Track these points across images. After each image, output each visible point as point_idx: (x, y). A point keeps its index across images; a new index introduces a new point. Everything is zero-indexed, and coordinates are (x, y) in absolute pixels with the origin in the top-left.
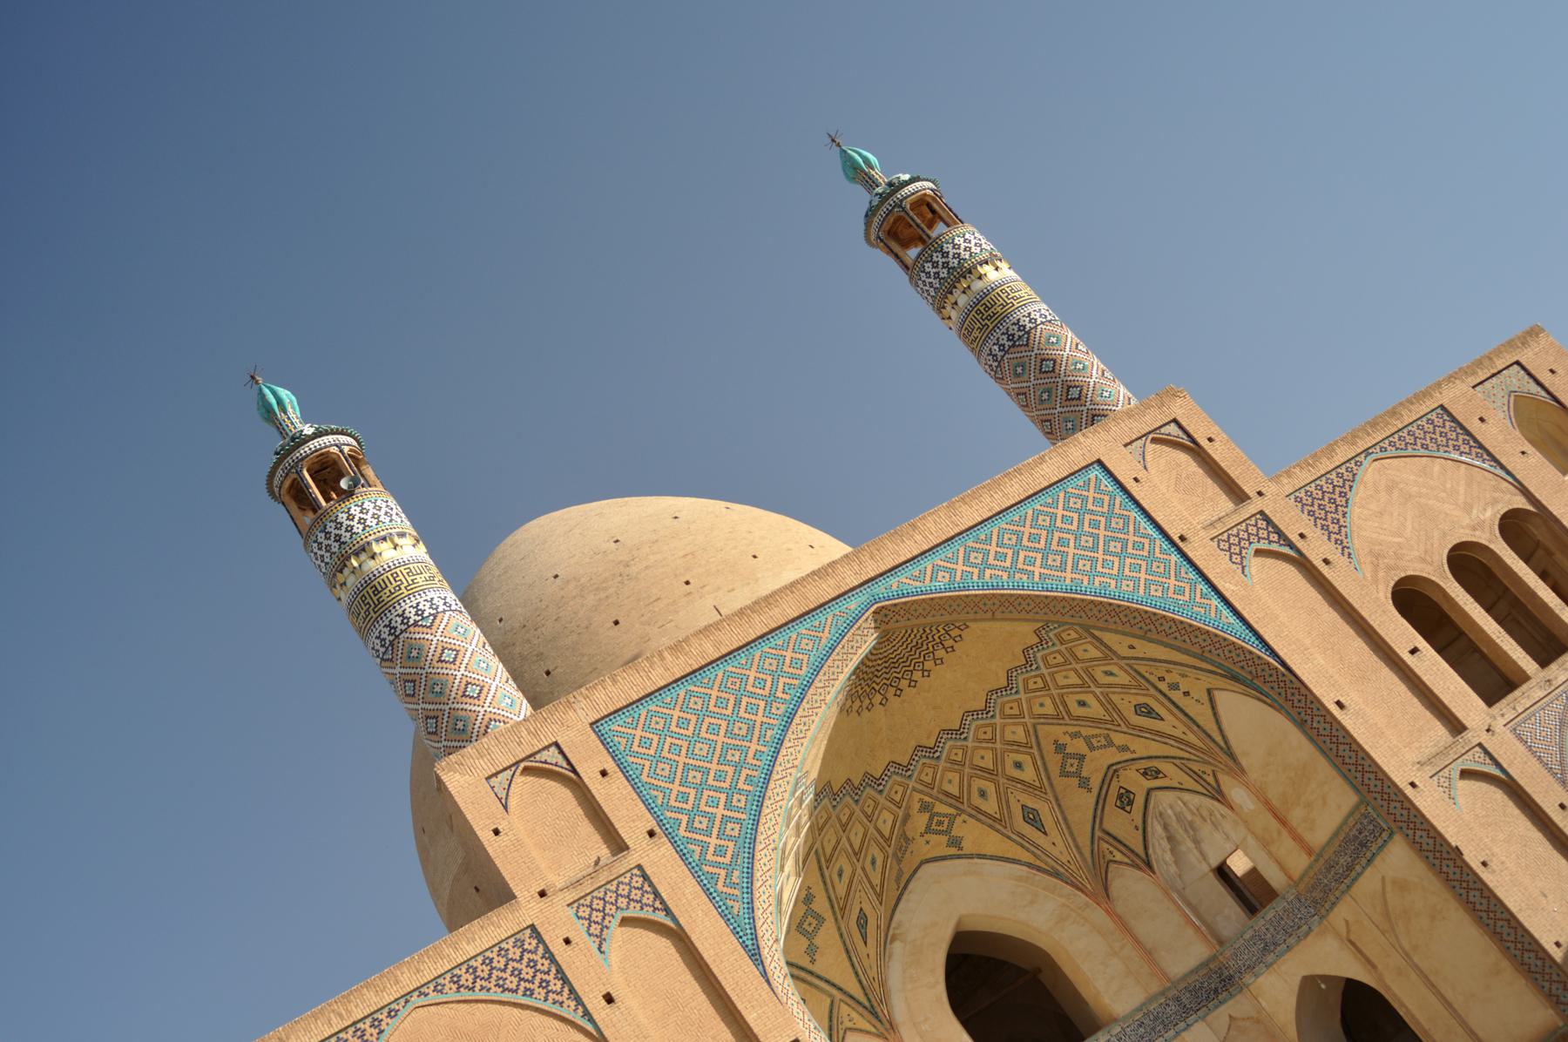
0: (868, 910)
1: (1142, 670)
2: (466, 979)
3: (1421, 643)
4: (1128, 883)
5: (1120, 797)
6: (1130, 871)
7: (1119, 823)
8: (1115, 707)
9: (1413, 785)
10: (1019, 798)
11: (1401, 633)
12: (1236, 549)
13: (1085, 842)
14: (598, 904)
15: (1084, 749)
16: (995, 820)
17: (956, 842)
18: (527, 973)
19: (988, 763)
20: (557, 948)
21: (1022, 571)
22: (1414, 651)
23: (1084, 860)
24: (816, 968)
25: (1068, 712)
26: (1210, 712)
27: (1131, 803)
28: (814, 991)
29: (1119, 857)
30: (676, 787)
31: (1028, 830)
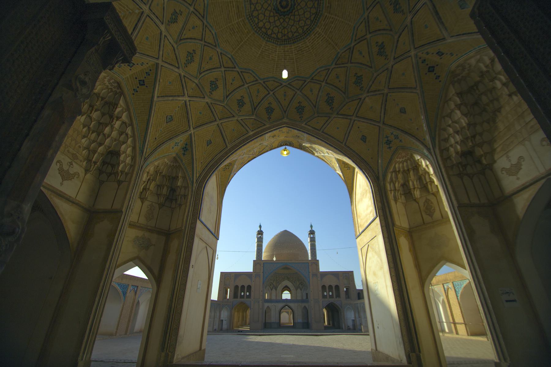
4: (299, 290)
7: (300, 286)
11: (320, 289)
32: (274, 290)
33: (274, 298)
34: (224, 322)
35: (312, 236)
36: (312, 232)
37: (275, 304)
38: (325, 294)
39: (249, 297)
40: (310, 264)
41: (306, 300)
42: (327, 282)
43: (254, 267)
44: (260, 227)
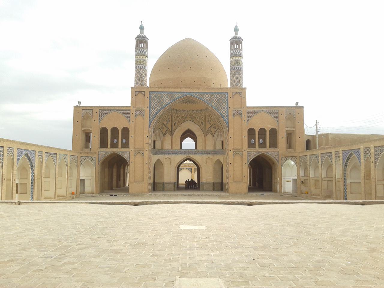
0: (176, 122)
2: (121, 111)
3: (247, 137)
4: (209, 136)
6: (211, 135)
7: (212, 129)
9: (230, 151)
11: (246, 134)
12: (235, 113)
14: (138, 111)
18: (127, 114)
19: (199, 115)
20: (131, 114)
21: (208, 101)
22: (245, 137)
27: (215, 128)
30: (154, 104)
31: (201, 124)
32: (168, 136)
33: (167, 147)
34: (87, 183)
35: (236, 46)
36: (236, 42)
37: (170, 156)
38: (253, 141)
39: (126, 145)
40: (230, 95)
41: (222, 151)
42: (257, 124)
43: (132, 98)
44: (142, 28)
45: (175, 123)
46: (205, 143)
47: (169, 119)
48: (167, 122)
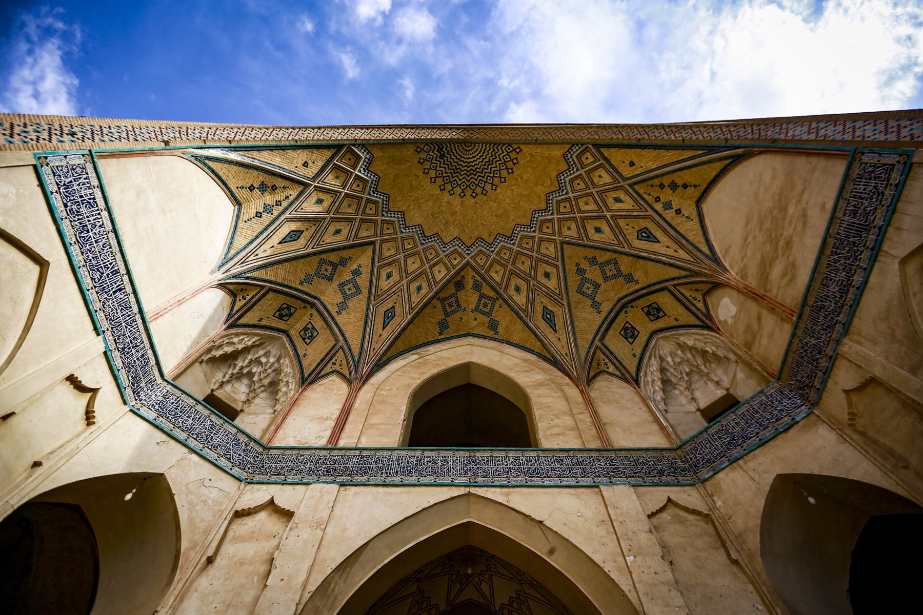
0: (398, 310)
1: (641, 192)
5: (625, 329)
8: (621, 231)
10: (542, 301)
13: (584, 345)
15: (600, 280)
16: (521, 309)
17: (493, 325)
23: (579, 356)
24: (339, 319)
25: (587, 236)
26: (698, 226)
27: (634, 337)
28: (328, 331)
29: (611, 369)
31: (543, 325)
45: (389, 315)
46: (595, 415)
47: (357, 273)
48: (339, 298)
